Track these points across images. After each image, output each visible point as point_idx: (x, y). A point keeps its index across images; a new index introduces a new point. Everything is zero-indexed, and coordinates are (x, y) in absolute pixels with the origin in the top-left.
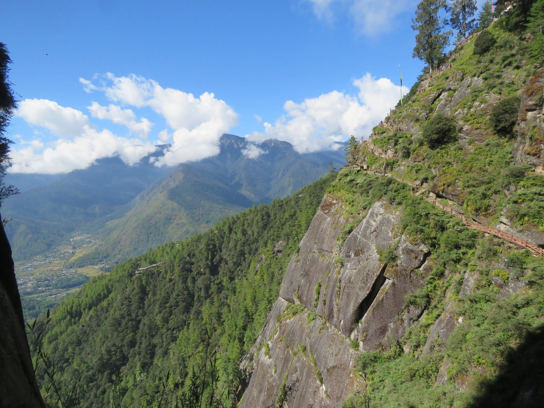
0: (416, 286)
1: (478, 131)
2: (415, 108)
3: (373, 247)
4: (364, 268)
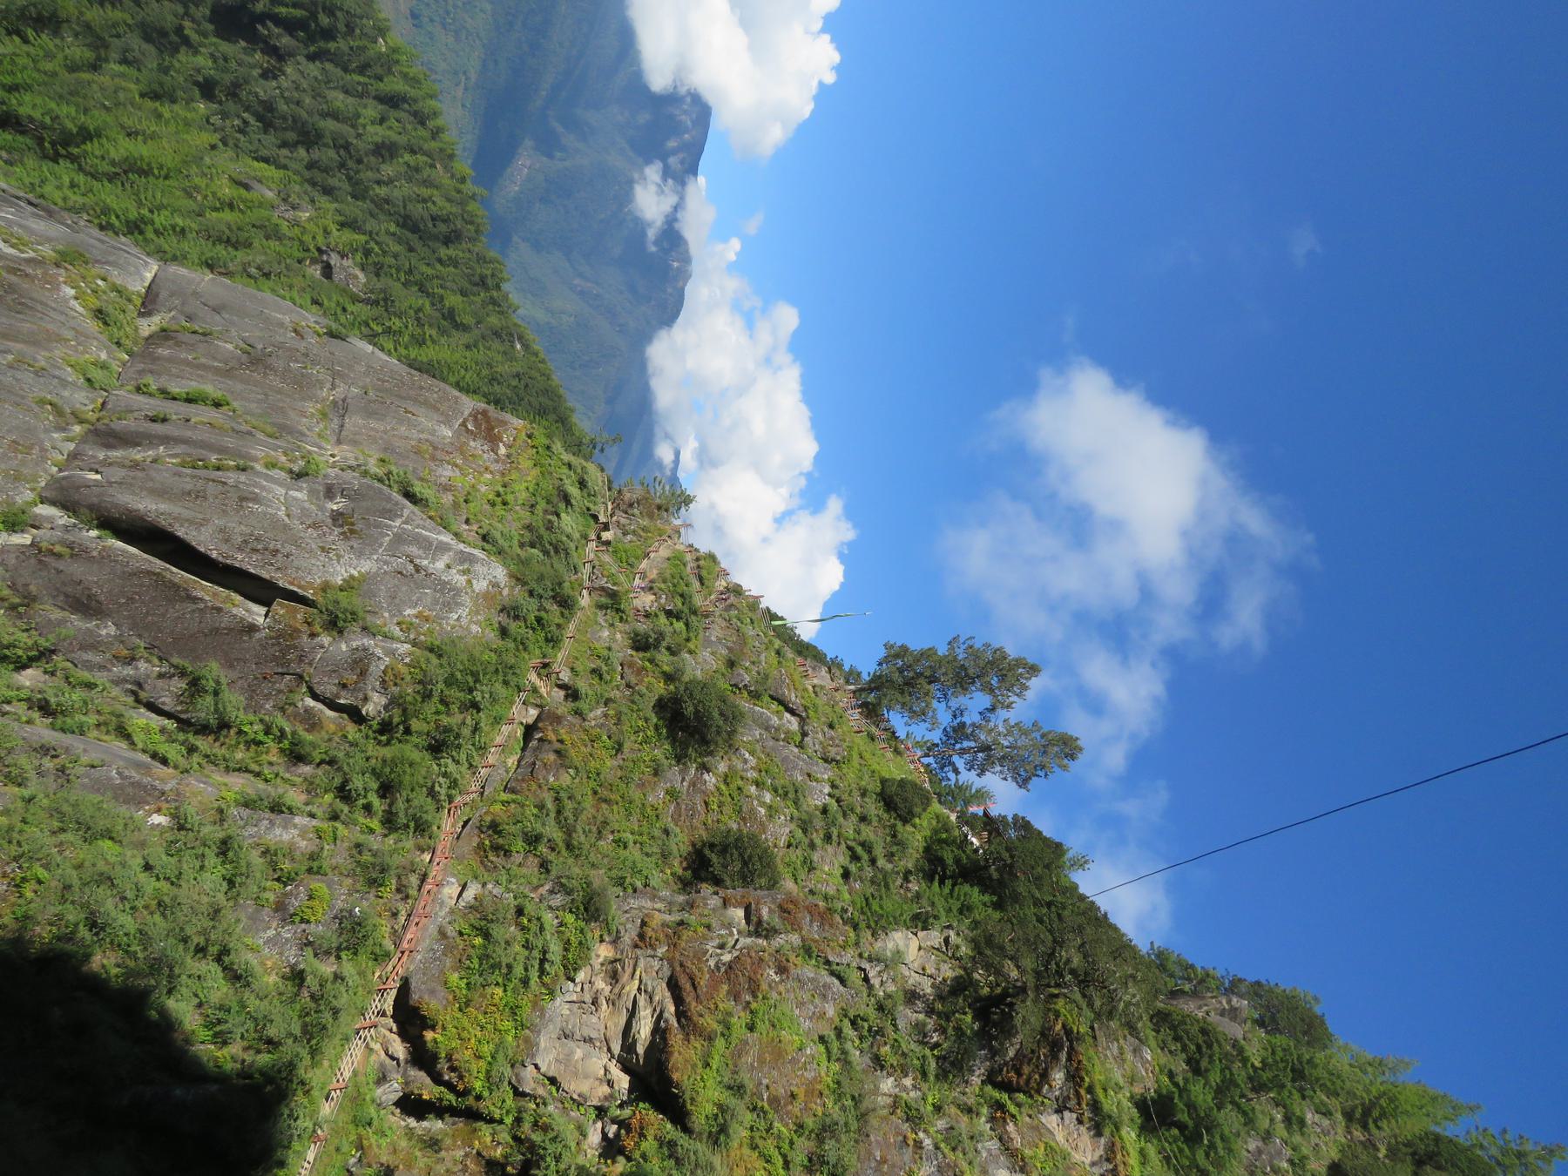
0: (251, 692)
1: (700, 808)
2: (763, 657)
3: (367, 566)
4: (296, 542)
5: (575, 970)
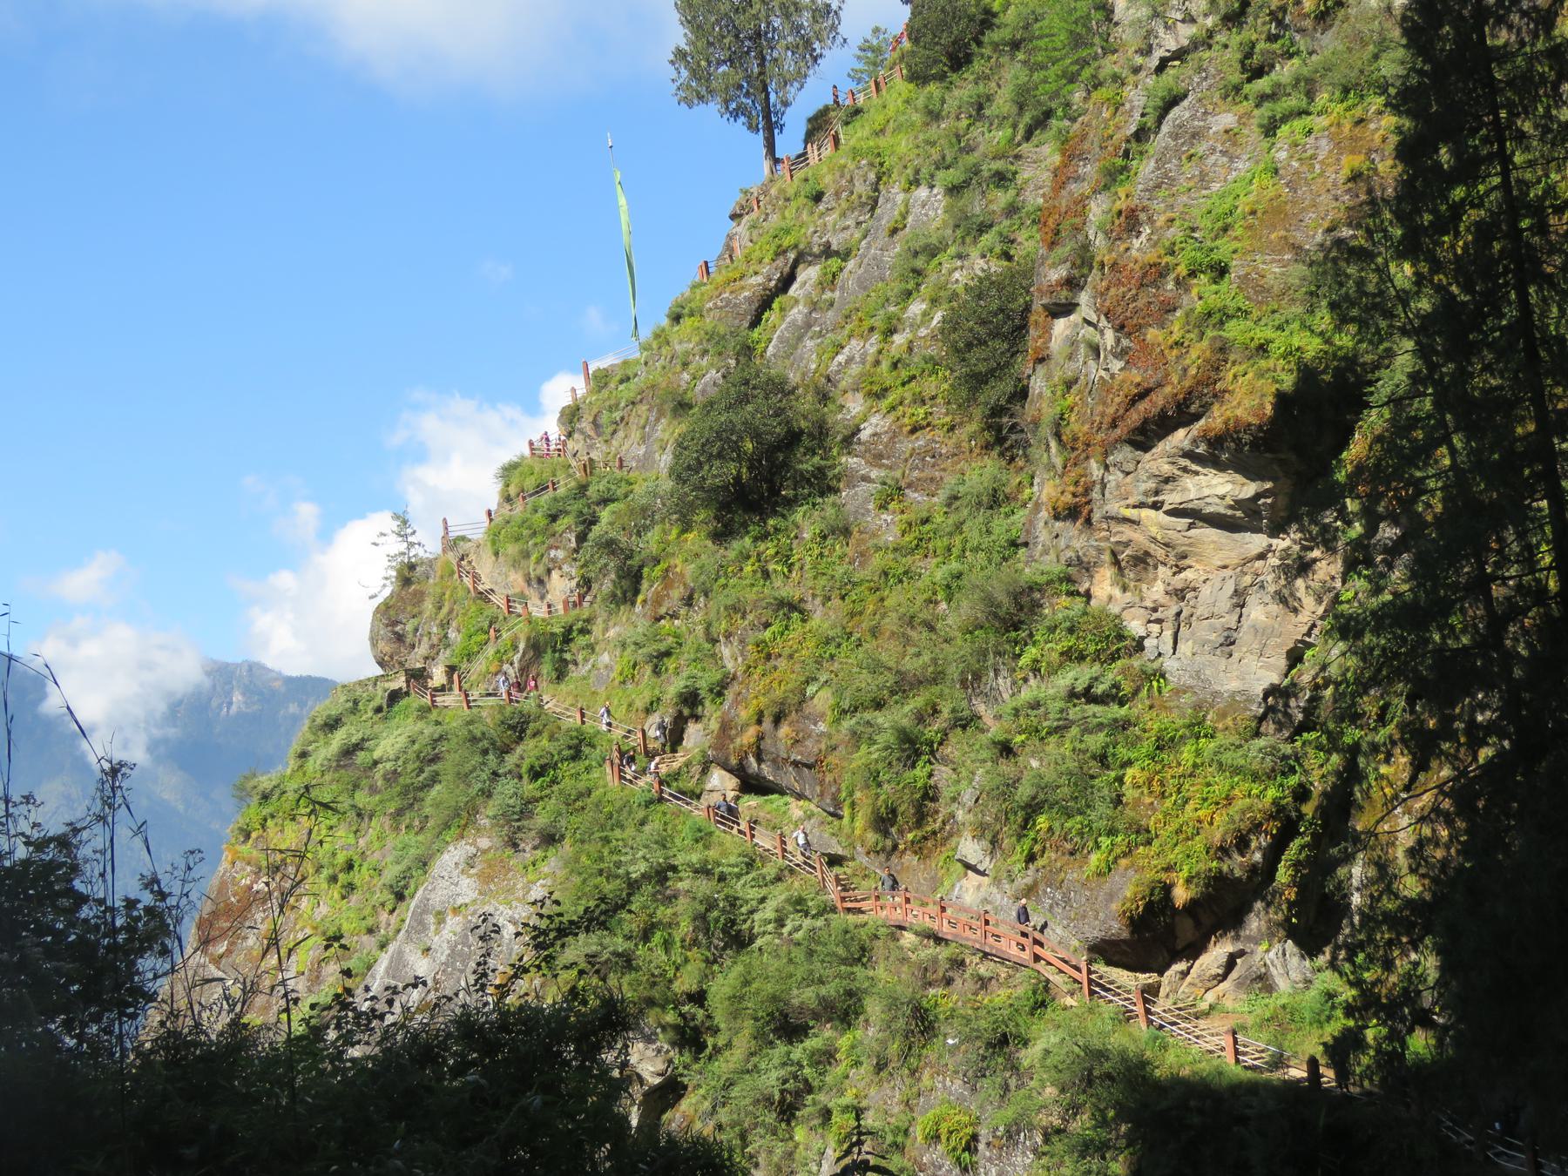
1: (920, 440)
5: (1121, 637)
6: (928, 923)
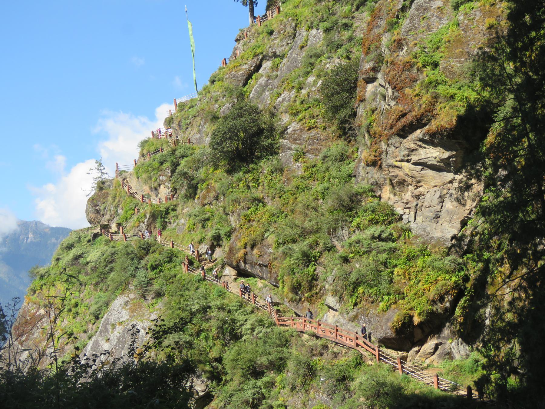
1: (312, 133)
5: (393, 214)
6: (313, 330)
